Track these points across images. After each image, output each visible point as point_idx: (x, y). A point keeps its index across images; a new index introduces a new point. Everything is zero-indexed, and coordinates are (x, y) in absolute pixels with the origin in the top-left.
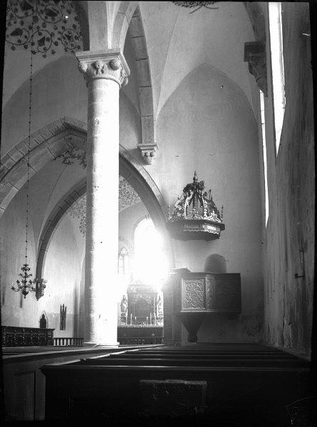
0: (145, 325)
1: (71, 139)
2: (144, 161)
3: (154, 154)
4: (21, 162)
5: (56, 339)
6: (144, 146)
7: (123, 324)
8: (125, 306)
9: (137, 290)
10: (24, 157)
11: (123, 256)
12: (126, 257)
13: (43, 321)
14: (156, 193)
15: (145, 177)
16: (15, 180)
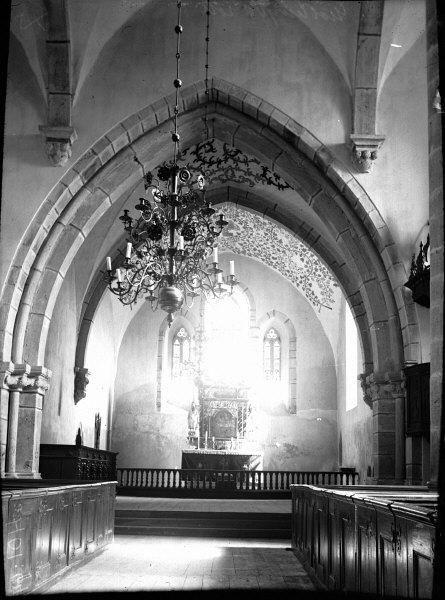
0: (219, 452)
1: (213, 120)
2: (358, 164)
3: (378, 154)
4: (125, 154)
5: (122, 470)
6: (362, 140)
7: (192, 449)
8: (196, 418)
9: (215, 394)
10: (129, 146)
11: (181, 340)
12: (186, 343)
13: (79, 439)
14: (377, 223)
15: (358, 194)
16: (112, 186)
